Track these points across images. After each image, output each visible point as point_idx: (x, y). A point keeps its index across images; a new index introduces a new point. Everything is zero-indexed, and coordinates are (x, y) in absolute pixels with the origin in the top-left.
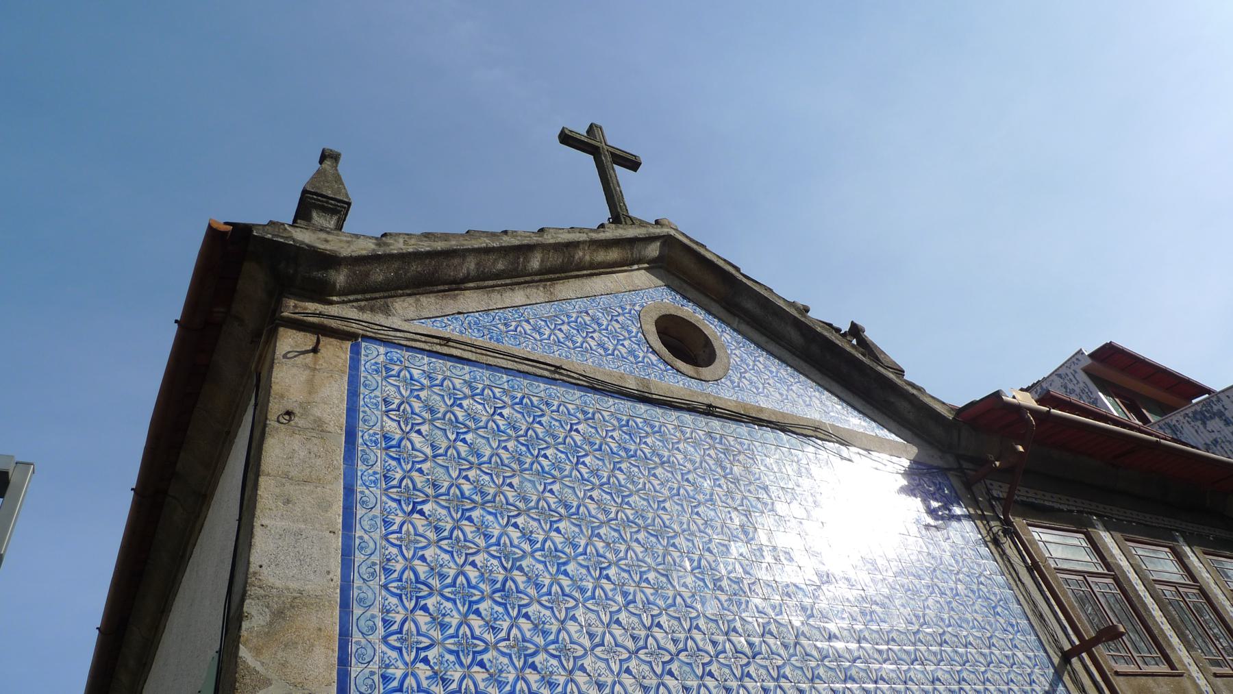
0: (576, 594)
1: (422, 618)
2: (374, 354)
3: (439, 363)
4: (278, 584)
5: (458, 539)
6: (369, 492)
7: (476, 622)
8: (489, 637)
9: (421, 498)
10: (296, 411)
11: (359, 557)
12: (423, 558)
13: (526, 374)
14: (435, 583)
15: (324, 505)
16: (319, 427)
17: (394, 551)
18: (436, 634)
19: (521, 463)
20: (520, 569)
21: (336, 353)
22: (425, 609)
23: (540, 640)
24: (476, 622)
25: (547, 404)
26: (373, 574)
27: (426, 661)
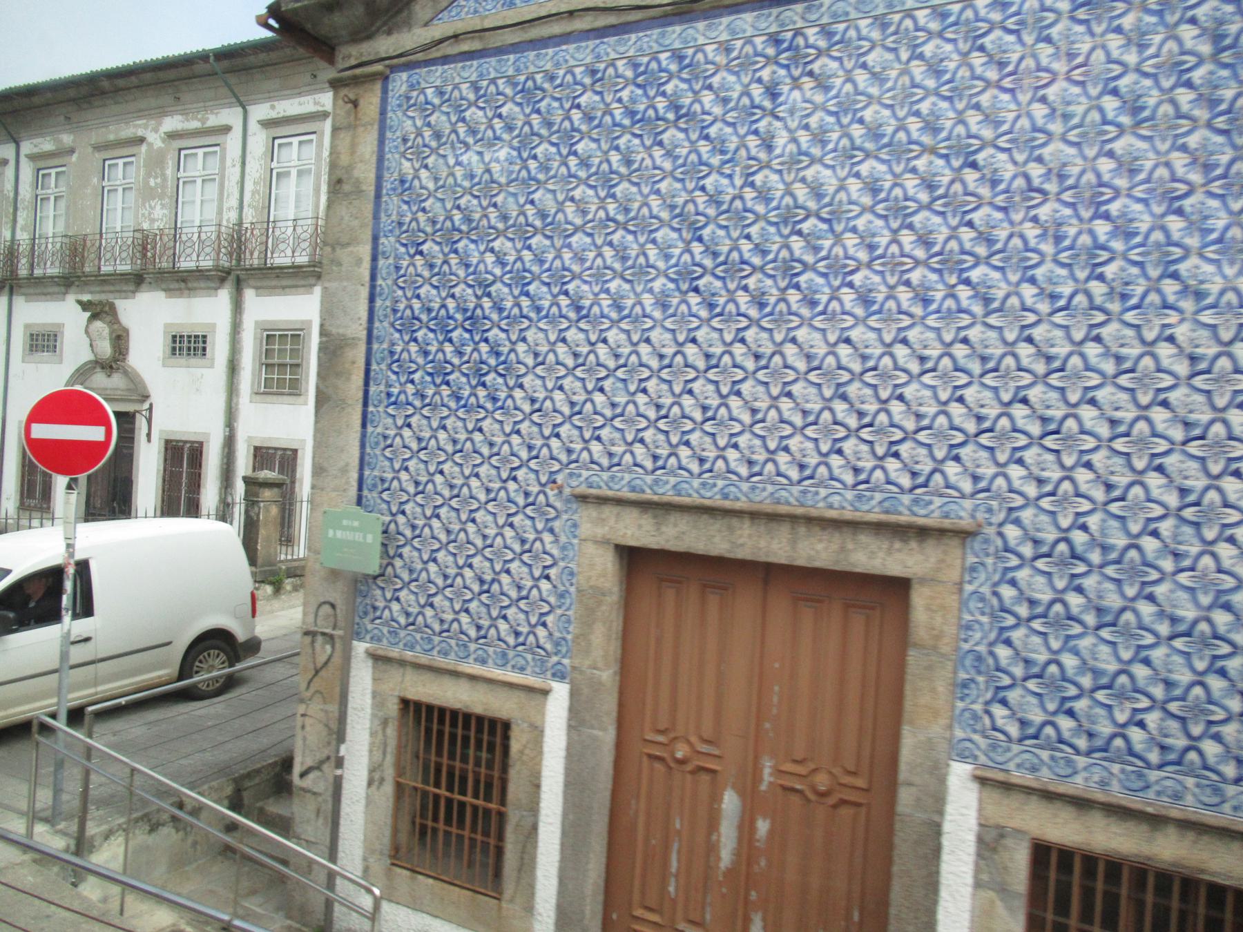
0: (533, 315)
1: (413, 348)
5: (445, 274)
6: (387, 243)
7: (448, 348)
10: (344, 177)
11: (378, 303)
14: (424, 317)
15: (359, 262)
17: (400, 293)
23: (492, 362)
24: (448, 348)
25: (552, 78)
26: (386, 316)
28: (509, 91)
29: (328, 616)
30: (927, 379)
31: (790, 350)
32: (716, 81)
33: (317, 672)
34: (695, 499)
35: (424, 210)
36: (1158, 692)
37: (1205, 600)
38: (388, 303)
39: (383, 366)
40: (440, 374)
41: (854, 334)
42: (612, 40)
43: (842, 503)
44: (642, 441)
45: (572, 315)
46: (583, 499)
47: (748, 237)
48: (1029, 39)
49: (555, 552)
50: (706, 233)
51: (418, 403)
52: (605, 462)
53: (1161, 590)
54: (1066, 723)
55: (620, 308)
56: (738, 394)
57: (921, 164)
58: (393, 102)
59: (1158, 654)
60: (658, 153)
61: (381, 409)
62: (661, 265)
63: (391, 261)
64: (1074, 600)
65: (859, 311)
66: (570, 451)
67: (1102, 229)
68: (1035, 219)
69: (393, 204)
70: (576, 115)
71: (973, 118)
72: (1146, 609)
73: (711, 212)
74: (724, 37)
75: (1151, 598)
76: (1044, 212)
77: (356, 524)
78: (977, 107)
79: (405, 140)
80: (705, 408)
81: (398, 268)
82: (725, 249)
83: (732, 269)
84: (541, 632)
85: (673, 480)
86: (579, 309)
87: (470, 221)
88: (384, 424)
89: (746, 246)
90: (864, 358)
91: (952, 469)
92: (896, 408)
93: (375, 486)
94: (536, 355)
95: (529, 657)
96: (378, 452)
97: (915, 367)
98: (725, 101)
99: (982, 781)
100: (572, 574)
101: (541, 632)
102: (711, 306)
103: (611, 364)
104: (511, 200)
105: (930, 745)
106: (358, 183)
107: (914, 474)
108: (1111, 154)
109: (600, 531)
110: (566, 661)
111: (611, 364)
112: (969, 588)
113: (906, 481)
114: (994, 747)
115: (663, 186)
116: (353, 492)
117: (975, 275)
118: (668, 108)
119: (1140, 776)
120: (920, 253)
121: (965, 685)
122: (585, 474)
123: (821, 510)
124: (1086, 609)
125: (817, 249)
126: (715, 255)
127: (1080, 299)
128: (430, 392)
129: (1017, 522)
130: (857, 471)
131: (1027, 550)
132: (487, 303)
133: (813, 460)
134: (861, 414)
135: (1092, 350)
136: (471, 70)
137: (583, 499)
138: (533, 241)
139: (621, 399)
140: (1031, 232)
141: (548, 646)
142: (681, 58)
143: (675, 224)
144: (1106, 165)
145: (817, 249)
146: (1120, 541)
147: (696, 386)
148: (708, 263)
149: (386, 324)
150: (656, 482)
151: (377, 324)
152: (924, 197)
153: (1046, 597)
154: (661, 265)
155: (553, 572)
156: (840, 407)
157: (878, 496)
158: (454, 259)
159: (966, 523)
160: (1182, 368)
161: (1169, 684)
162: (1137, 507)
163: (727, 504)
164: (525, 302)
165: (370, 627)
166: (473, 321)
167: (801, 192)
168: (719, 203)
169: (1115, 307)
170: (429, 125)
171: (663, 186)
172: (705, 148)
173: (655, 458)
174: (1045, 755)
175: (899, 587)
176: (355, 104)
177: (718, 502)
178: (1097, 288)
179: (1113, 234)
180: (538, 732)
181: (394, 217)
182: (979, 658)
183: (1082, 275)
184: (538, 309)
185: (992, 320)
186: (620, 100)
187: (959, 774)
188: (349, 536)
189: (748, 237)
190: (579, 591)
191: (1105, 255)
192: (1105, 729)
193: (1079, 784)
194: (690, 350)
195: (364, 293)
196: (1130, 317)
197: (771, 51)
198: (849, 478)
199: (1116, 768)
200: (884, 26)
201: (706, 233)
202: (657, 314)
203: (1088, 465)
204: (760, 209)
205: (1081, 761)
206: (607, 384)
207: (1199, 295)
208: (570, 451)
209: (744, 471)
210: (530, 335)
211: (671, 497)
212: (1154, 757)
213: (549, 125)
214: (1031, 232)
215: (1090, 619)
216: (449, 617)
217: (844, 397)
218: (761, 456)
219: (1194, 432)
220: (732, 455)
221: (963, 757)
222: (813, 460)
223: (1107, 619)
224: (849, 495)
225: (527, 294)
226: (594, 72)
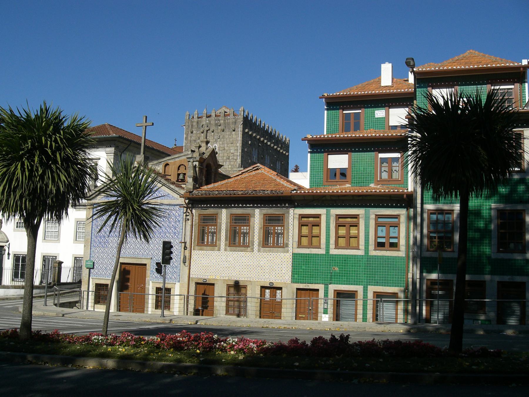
88: (93, 249)
99: (152, 282)
105: (148, 279)
175: (145, 265)
187: (151, 282)
188: (89, 263)
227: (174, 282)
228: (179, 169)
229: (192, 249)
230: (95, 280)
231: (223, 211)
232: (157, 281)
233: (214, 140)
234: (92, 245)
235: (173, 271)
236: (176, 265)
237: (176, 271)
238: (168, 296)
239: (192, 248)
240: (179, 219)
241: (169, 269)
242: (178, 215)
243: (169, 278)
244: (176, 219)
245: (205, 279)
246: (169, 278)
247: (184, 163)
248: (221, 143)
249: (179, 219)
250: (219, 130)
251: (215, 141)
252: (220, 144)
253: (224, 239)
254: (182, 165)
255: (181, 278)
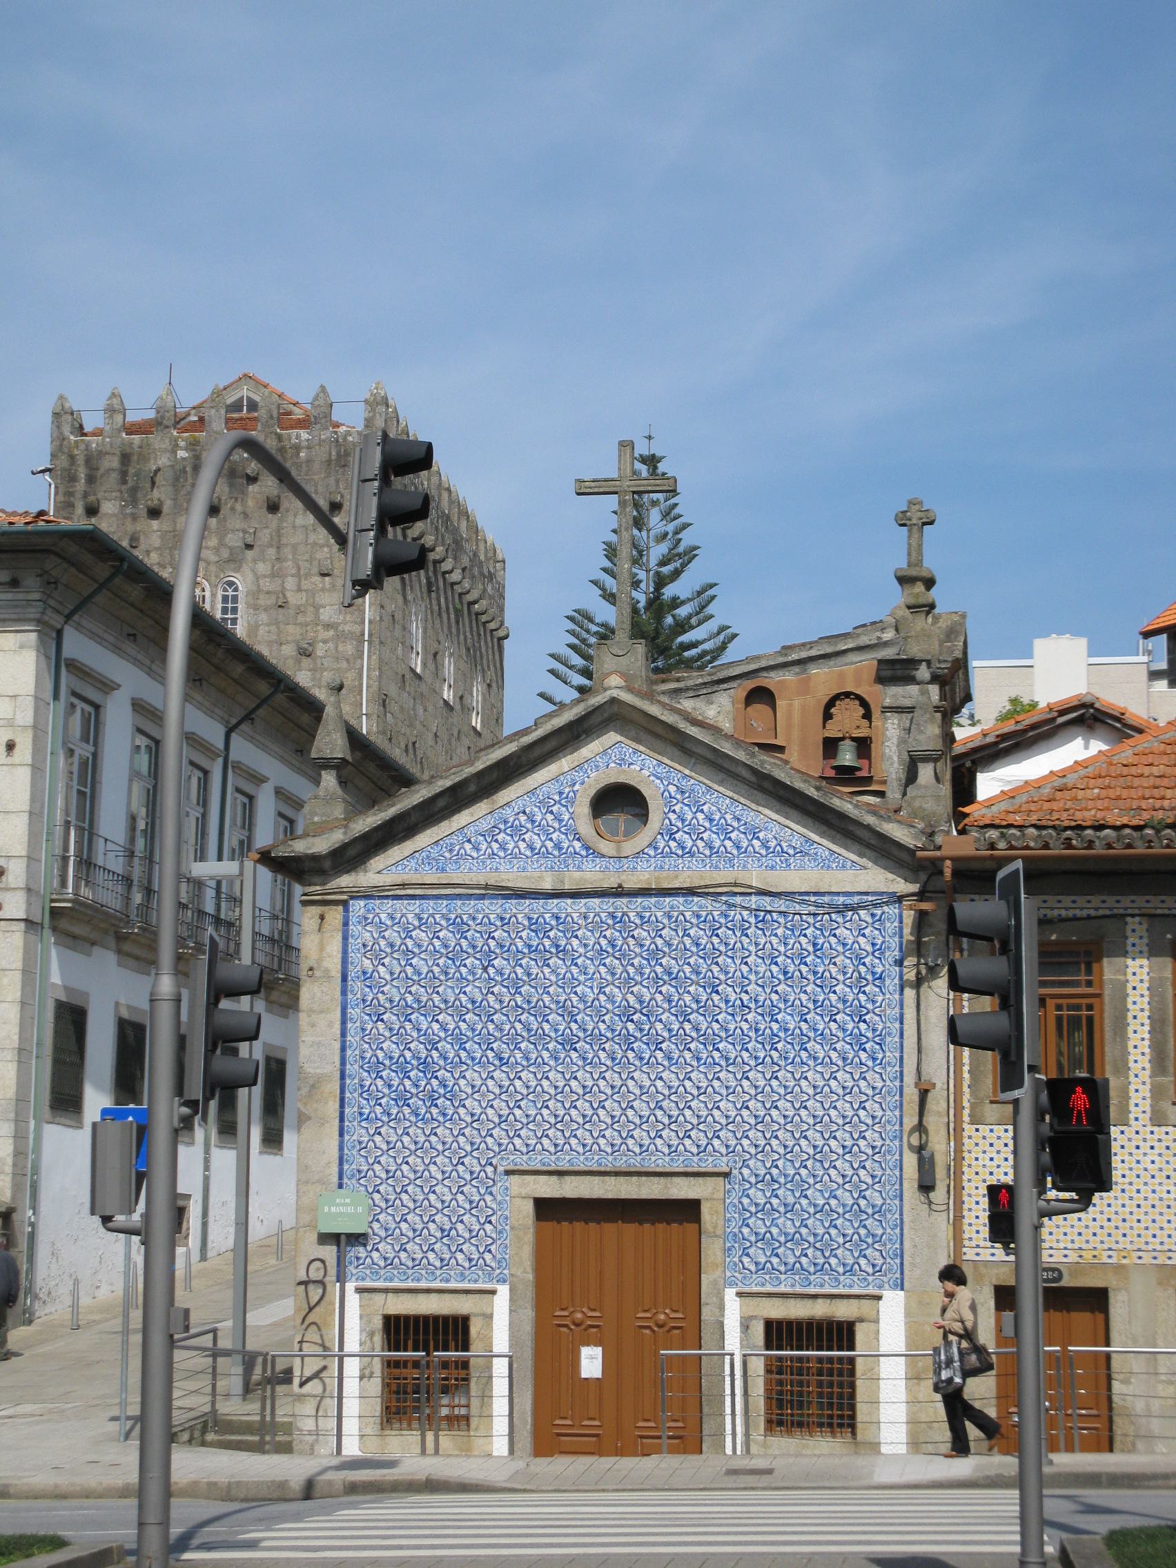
0: (469, 1062)
1: (379, 1082)
2: (358, 906)
3: (398, 903)
4: (312, 1071)
7: (407, 1083)
8: (414, 1091)
9: (382, 1010)
10: (315, 966)
11: (349, 1052)
12: (382, 1049)
13: (459, 897)
14: (387, 1062)
16: (327, 976)
17: (366, 1046)
18: (386, 1091)
19: (446, 974)
20: (437, 1049)
21: (335, 915)
22: (381, 1077)
23: (442, 1091)
24: (407, 1083)
25: (474, 919)
27: (380, 1105)
28: (443, 923)
29: (318, 1269)
30: (701, 1098)
31: (630, 1083)
32: (580, 933)
33: (311, 1309)
34: (582, 1168)
35: (383, 992)
36: (811, 1239)
37: (827, 1195)
38: (357, 1052)
39: (356, 1095)
40: (402, 1099)
41: (664, 1075)
42: (514, 901)
43: (663, 1164)
44: (547, 1136)
45: (497, 1062)
46: (508, 1173)
47: (603, 1021)
48: (738, 934)
49: (494, 1206)
50: (579, 1018)
51: (385, 1119)
52: (524, 1150)
53: (809, 1193)
54: (775, 1260)
55: (528, 1059)
56: (604, 1107)
57: (692, 989)
58: (353, 920)
59: (810, 1222)
60: (546, 970)
61: (355, 1123)
62: (553, 1034)
63: (358, 1024)
64: (775, 1201)
65: (666, 1063)
66: (500, 1145)
67: (775, 1026)
68: (746, 1021)
69: (356, 986)
70: (492, 943)
71: (715, 969)
72: (804, 1202)
73: (581, 1006)
74: (583, 910)
75: (806, 1197)
76: (750, 1017)
77: (348, 1201)
78: (717, 964)
79: (364, 945)
80: (584, 1116)
81: (363, 1030)
82: (591, 1028)
83: (596, 1039)
84: (488, 1256)
85: (568, 1158)
86: (501, 1059)
87: (419, 1001)
88: (358, 1132)
89: (602, 1026)
90: (670, 1088)
91: (716, 1142)
92: (688, 1113)
93: (353, 1176)
94: (473, 1087)
95: (480, 1273)
96: (355, 1152)
97: (695, 1092)
98: (586, 946)
99: (740, 1294)
100: (506, 1218)
101: (488, 1256)
102: (584, 1059)
103: (525, 1092)
104: (449, 990)
106: (327, 971)
107: (698, 1146)
108: (776, 992)
109: (524, 1192)
110: (506, 1272)
111: (525, 1092)
112: (728, 1201)
113: (695, 1150)
114: (745, 1278)
115: (551, 990)
116: (335, 1179)
117: (721, 1046)
118: (551, 946)
119: (807, 1279)
120: (694, 1034)
121: (729, 1249)
122: (512, 1157)
123: (653, 1168)
124: (779, 1205)
125: (641, 1030)
126: (585, 1030)
127: (768, 1059)
128: (394, 1111)
129: (748, 1166)
130: (669, 1146)
131: (753, 1180)
132: (435, 1054)
133: (646, 1142)
134: (670, 1117)
135: (774, 1083)
136: (415, 905)
137: (508, 1173)
138: (467, 1017)
139: (532, 1112)
140: (745, 1026)
141: (493, 1264)
142: (558, 918)
143: (560, 1011)
144: (775, 997)
145: (641, 1030)
146: (792, 1172)
147: (578, 1104)
148: (581, 1034)
149: (356, 1066)
150: (558, 1159)
151: (348, 1066)
152: (694, 1006)
153: (762, 1201)
154: (553, 1034)
155: (493, 1219)
156: (659, 1113)
157: (682, 1159)
158: (408, 1026)
159: (726, 1169)
160: (811, 1091)
161: (815, 1235)
162: (797, 1156)
163: (602, 1169)
164: (463, 1054)
165: (354, 1271)
166: (425, 1065)
167: (631, 999)
168: (585, 1002)
169: (782, 1063)
170: (384, 937)
171: (551, 990)
172: (575, 970)
173: (556, 1145)
174: (767, 1277)
176: (322, 918)
177: (595, 1168)
178: (775, 1054)
179: (780, 1029)
180: (489, 1317)
181: (359, 996)
182: (735, 1235)
183: (768, 1048)
184: (473, 1059)
185: (730, 1068)
186: (521, 938)
187: (730, 1294)
189: (603, 1021)
190: (512, 1228)
191: (777, 1039)
192: (791, 1260)
193: (782, 1289)
194: (574, 1083)
195: (337, 1045)
196: (789, 1068)
197: (610, 922)
198: (666, 1150)
199: (797, 1277)
200: (670, 917)
201: (579, 1018)
202: (552, 1063)
203: (776, 1137)
204: (609, 1006)
205: (783, 1277)
206: (523, 1104)
207: (815, 1059)
208: (500, 1145)
209: (609, 1150)
210: (468, 1074)
211: (567, 1167)
212: (812, 1269)
213: (474, 947)
214: (745, 1026)
215: (782, 1209)
216: (419, 1256)
217: (661, 1108)
218: (618, 1141)
219: (818, 1120)
220: (602, 1141)
221: (731, 1285)
222: (646, 1142)
223: (789, 1208)
224: (667, 1159)
225: (465, 1049)
226: (502, 919)
227: (871, 1290)
228: (827, 716)
229: (966, 1118)
230: (379, 1298)
231: (1129, 928)
232: (769, 1288)
233: (225, 554)
234: (347, 1110)
235: (863, 1232)
236: (879, 1202)
237: (880, 1232)
238: (840, 1359)
239: (966, 1112)
240: (879, 970)
241: (839, 1222)
242: (869, 949)
243: (841, 1270)
244: (862, 969)
245: (1053, 1270)
246: (841, 1270)
247: (858, 683)
248: (262, 568)
249: (879, 970)
250: (250, 503)
251: (229, 561)
252: (257, 578)
253: (1148, 1066)
254: (847, 695)
255: (913, 1264)
